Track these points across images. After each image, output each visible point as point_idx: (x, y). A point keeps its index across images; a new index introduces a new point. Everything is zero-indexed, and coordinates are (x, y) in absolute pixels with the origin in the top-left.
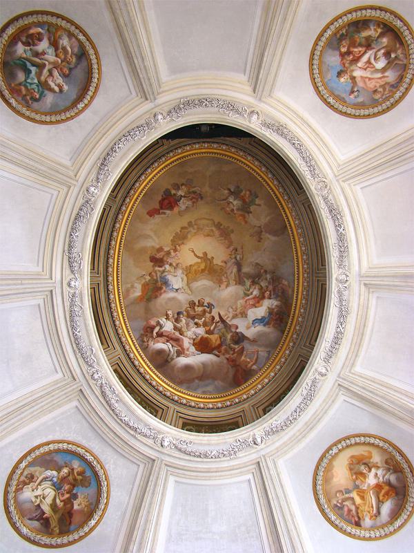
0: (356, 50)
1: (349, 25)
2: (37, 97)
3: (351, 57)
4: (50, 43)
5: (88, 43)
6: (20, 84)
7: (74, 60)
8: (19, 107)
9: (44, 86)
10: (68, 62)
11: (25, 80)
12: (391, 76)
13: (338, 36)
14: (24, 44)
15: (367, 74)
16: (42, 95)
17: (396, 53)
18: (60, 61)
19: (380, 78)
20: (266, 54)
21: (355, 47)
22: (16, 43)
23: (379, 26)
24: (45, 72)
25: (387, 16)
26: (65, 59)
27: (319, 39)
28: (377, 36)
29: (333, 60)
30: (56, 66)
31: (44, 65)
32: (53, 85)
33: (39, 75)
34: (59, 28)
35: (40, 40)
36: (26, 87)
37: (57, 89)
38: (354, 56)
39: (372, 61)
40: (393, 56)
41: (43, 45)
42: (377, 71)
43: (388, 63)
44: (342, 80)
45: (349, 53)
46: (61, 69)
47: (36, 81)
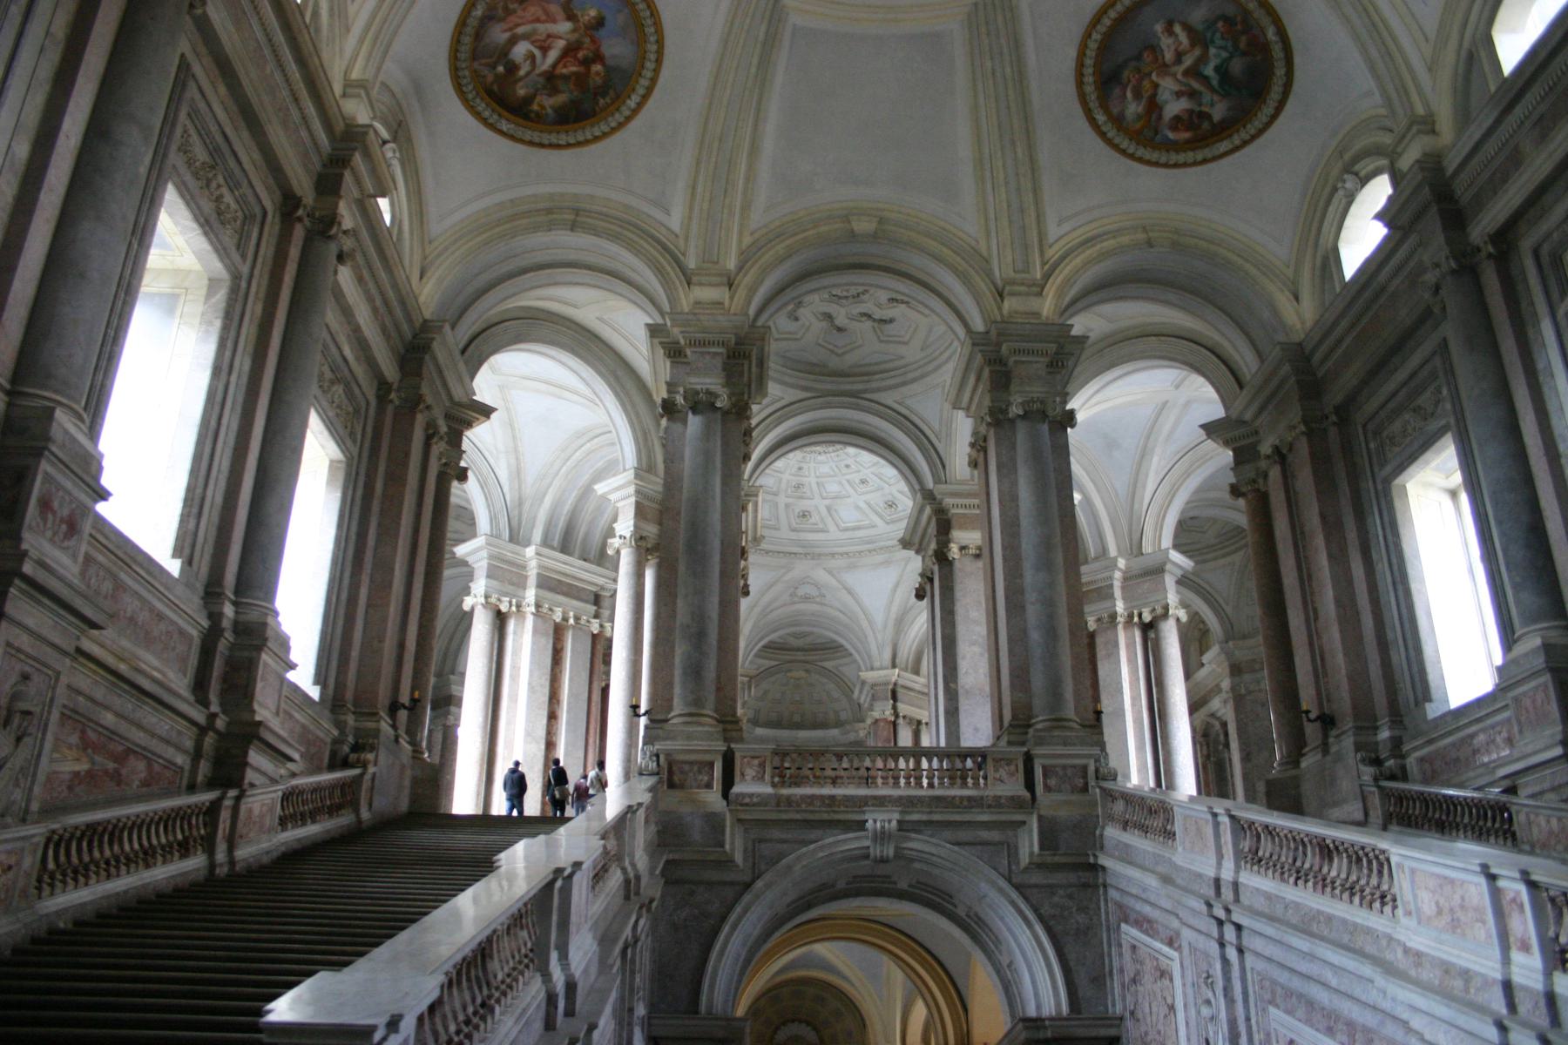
0: (574, 69)
1: (594, 114)
2: (1220, 24)
3: (580, 55)
4: (1161, 109)
5: (1091, 105)
6: (1245, 54)
7: (1126, 74)
8: (1265, 21)
9: (1197, 38)
10: (1139, 70)
11: (1231, 57)
12: (498, 34)
13: (612, 92)
14: (1208, 117)
15: (543, 28)
16: (1210, 24)
17: (496, 76)
18: (1154, 77)
19: (518, 25)
20: (753, 70)
21: (574, 73)
22: (1223, 121)
23: (537, 114)
24: (1188, 61)
25: (528, 135)
26: (1140, 80)
27: (649, 90)
28: (538, 99)
29: (616, 49)
30: (1164, 69)
31: (1186, 73)
32: (1183, 38)
33: (1203, 59)
34: (1137, 136)
35: (1177, 118)
36: (1236, 46)
37: (1177, 29)
38: (575, 57)
39: (537, 53)
40: (501, 69)
41: (1174, 107)
42: (525, 37)
43: (506, 55)
44: (593, 13)
45: (586, 63)
46: (1156, 59)
47: (1212, 51)
